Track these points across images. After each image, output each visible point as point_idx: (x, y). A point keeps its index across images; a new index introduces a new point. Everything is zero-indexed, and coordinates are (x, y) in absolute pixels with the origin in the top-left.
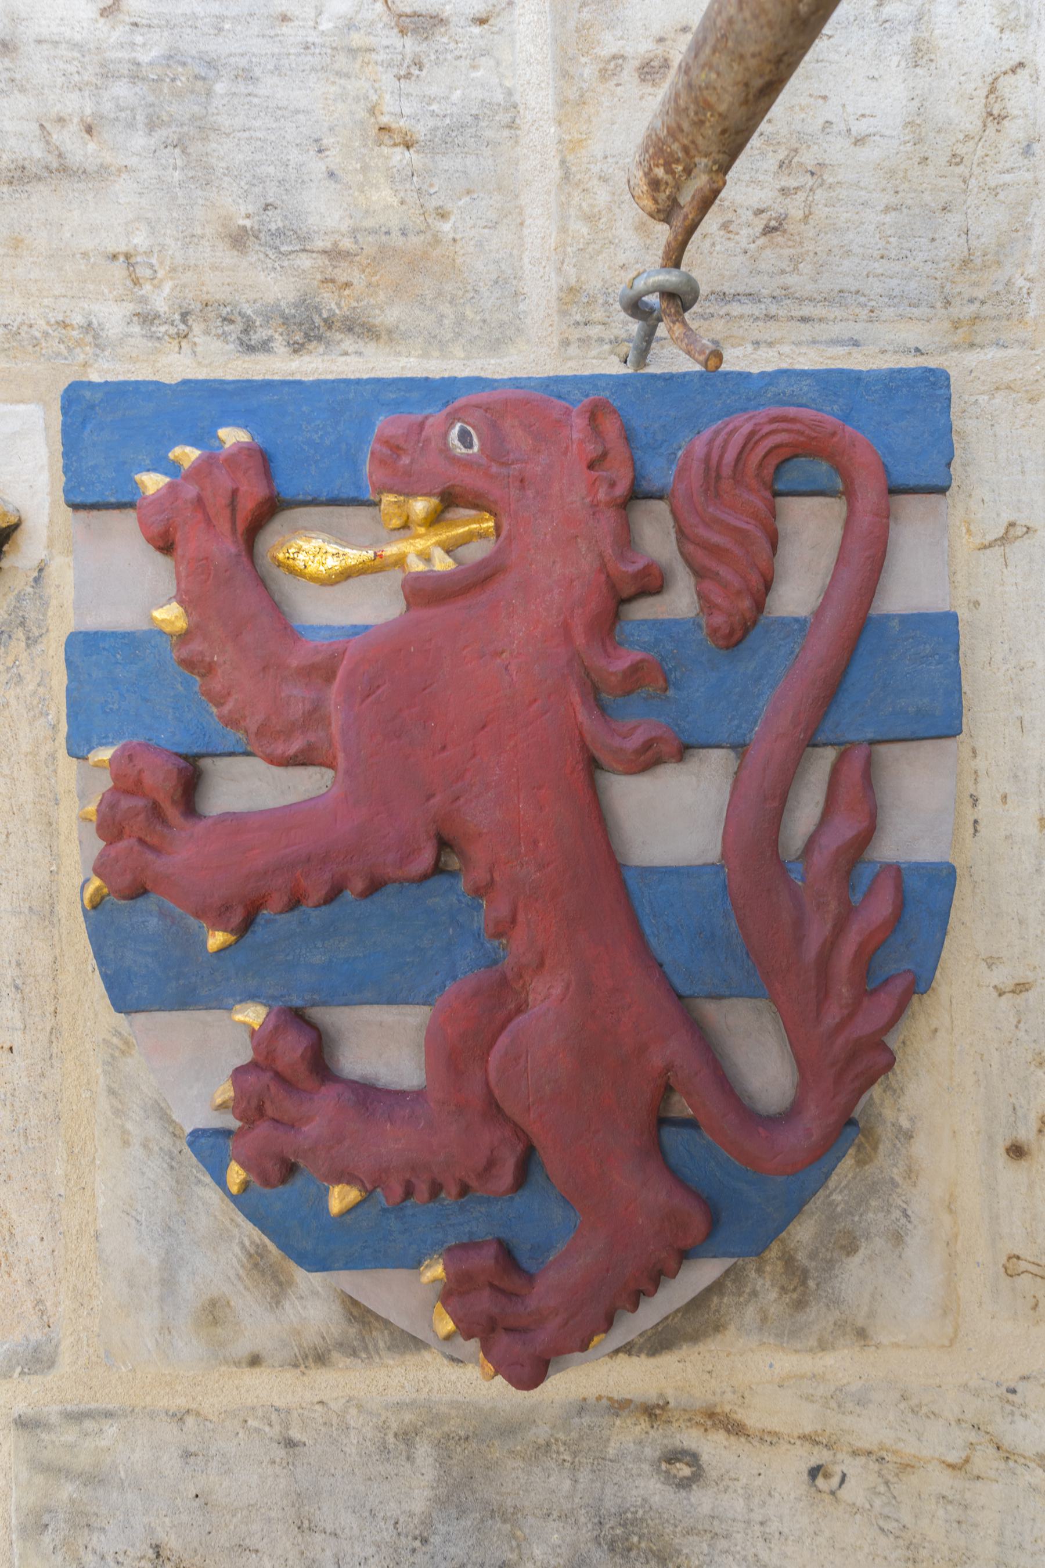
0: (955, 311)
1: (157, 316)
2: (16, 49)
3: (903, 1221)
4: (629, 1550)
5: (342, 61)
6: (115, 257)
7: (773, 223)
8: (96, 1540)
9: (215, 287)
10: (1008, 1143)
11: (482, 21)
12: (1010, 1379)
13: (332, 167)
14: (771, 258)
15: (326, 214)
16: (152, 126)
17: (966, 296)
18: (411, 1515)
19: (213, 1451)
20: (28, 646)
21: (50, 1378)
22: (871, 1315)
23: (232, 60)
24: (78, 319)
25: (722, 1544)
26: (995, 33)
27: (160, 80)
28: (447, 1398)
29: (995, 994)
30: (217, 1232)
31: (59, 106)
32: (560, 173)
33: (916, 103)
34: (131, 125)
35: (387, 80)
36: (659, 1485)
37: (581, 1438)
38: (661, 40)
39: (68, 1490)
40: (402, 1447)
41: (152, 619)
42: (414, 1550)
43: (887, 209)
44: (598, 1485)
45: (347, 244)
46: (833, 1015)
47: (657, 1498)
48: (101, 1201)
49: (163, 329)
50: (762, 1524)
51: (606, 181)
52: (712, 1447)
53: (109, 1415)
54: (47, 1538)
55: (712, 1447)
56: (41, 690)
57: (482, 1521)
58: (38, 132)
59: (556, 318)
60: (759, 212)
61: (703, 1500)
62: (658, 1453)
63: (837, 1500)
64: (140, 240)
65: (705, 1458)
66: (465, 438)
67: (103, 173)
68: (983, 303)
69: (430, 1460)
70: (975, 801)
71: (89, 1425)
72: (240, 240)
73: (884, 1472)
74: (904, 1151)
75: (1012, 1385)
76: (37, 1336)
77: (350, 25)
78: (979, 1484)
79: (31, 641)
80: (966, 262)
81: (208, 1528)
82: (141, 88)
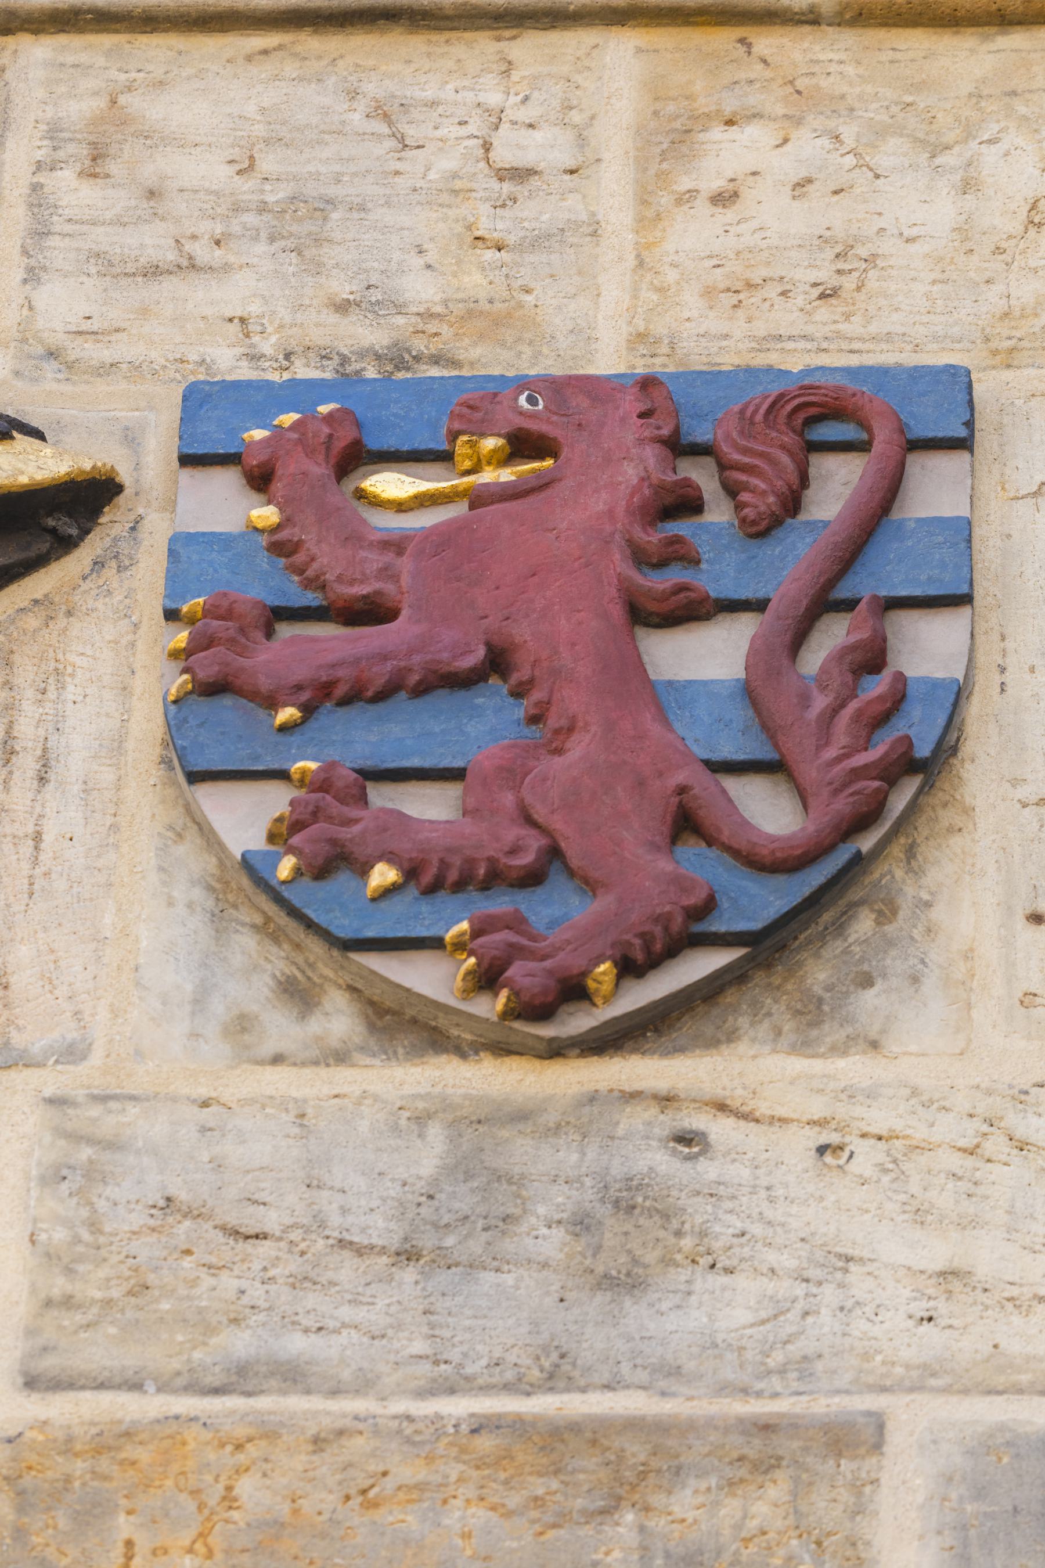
0: (994, 345)
1: (263, 356)
2: (160, 194)
3: (920, 966)
4: (634, 1207)
5: (445, 198)
6: (231, 320)
7: (828, 292)
8: (110, 1191)
9: (318, 337)
10: (1028, 912)
11: (572, 172)
12: (1024, 1083)
13: (430, 262)
14: (824, 313)
15: (421, 289)
16: (272, 239)
17: (1005, 335)
18: (420, 1178)
19: (230, 1127)
20: (119, 571)
21: (81, 1069)
22: (883, 1031)
23: (348, 199)
24: (194, 357)
25: (728, 1205)
26: (1037, 172)
27: (284, 211)
28: (462, 1091)
29: (1019, 806)
30: (251, 966)
31: (193, 229)
32: (635, 263)
33: (964, 217)
34: (256, 239)
35: (485, 209)
36: (666, 1157)
37: (591, 1122)
38: (732, 180)
39: (86, 1153)
40: (414, 1127)
41: (249, 520)
42: (419, 1204)
43: (934, 282)
44: (606, 1157)
45: (438, 309)
46: (831, 753)
47: (664, 1167)
48: (144, 943)
49: (267, 364)
50: (768, 1189)
51: (676, 266)
52: (720, 1130)
53: (133, 1098)
54: (64, 1186)
55: (720, 1130)
56: (127, 601)
57: (489, 1183)
58: (173, 244)
59: (624, 352)
60: (815, 285)
61: (708, 1170)
62: (666, 1133)
63: (844, 1172)
64: (254, 308)
65: (712, 1138)
66: (532, 400)
67: (227, 268)
68: (1020, 340)
69: (441, 1138)
70: (1003, 670)
71: (113, 1105)
72: (343, 307)
73: (893, 1152)
74: (923, 916)
75: (1025, 1088)
76: (73, 1035)
77: (455, 176)
78: (989, 1165)
79: (120, 569)
80: (1006, 314)
81: (219, 1184)
82: (266, 217)
